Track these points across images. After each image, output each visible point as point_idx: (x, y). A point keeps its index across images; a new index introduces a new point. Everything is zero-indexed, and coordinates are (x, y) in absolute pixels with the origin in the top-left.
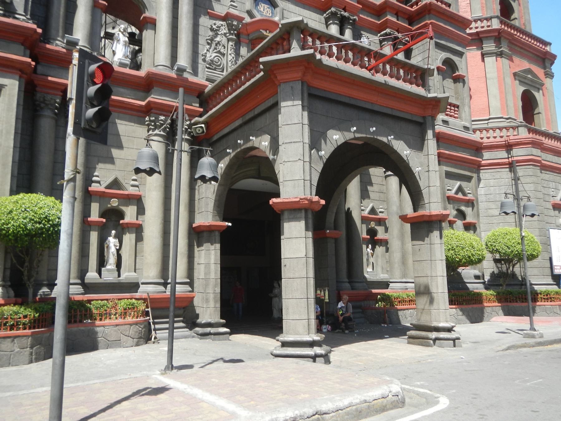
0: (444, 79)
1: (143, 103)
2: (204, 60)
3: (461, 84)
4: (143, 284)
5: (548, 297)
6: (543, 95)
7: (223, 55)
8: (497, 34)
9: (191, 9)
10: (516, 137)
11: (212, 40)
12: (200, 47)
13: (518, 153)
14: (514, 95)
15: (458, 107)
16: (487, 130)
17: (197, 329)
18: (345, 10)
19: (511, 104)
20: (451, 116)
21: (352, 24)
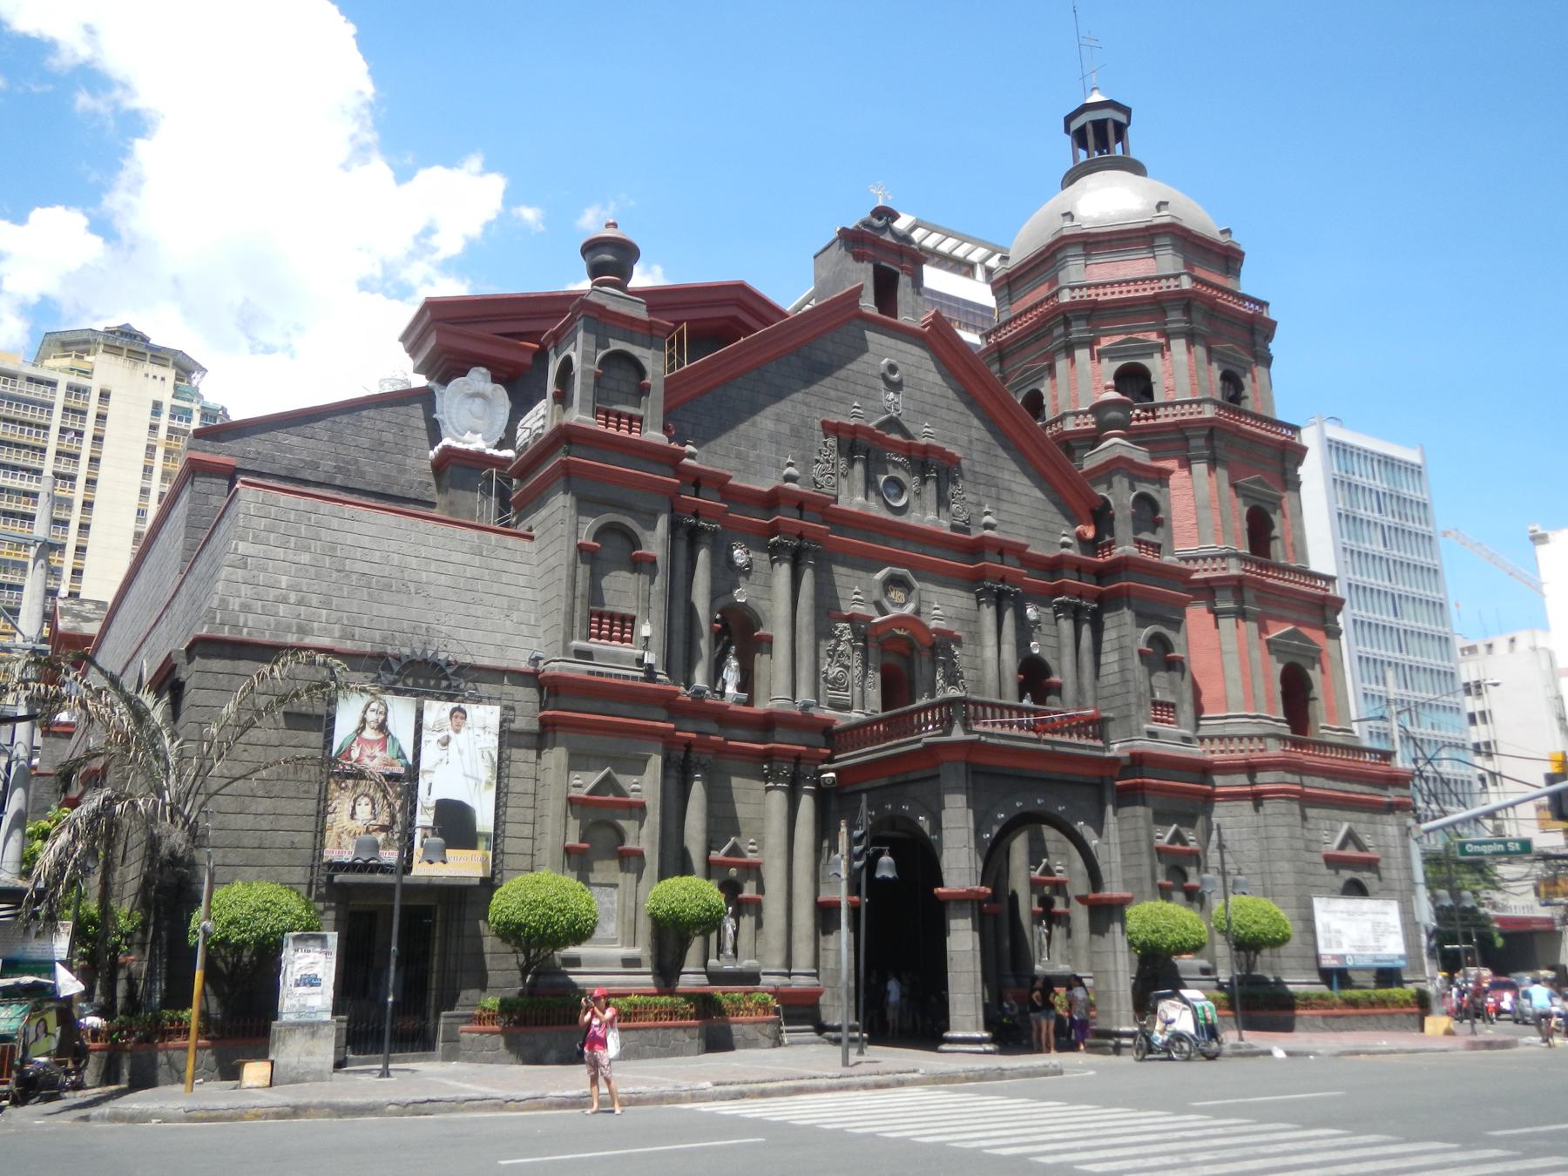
0: (1151, 674)
1: (761, 747)
2: (826, 680)
3: (1177, 675)
4: (765, 974)
5: (1309, 1002)
6: (1323, 671)
7: (847, 668)
8: (1235, 583)
9: (812, 620)
10: (1261, 754)
11: (835, 650)
12: (821, 661)
13: (1266, 780)
14: (1267, 676)
15: (1173, 706)
16: (1221, 738)
17: (828, 1034)
18: (1003, 580)
19: (1260, 692)
20: (1162, 721)
21: (1013, 599)
